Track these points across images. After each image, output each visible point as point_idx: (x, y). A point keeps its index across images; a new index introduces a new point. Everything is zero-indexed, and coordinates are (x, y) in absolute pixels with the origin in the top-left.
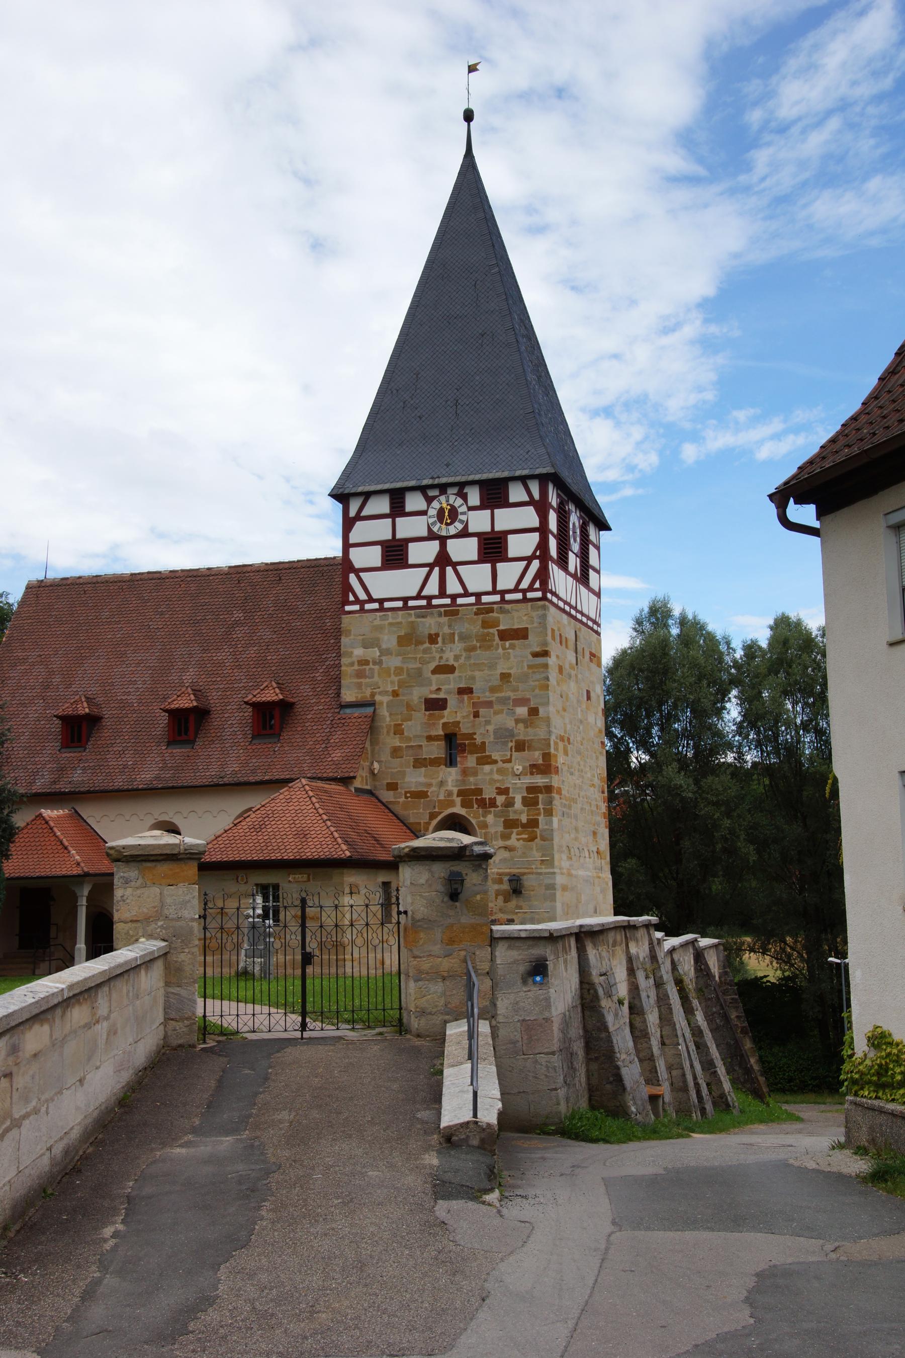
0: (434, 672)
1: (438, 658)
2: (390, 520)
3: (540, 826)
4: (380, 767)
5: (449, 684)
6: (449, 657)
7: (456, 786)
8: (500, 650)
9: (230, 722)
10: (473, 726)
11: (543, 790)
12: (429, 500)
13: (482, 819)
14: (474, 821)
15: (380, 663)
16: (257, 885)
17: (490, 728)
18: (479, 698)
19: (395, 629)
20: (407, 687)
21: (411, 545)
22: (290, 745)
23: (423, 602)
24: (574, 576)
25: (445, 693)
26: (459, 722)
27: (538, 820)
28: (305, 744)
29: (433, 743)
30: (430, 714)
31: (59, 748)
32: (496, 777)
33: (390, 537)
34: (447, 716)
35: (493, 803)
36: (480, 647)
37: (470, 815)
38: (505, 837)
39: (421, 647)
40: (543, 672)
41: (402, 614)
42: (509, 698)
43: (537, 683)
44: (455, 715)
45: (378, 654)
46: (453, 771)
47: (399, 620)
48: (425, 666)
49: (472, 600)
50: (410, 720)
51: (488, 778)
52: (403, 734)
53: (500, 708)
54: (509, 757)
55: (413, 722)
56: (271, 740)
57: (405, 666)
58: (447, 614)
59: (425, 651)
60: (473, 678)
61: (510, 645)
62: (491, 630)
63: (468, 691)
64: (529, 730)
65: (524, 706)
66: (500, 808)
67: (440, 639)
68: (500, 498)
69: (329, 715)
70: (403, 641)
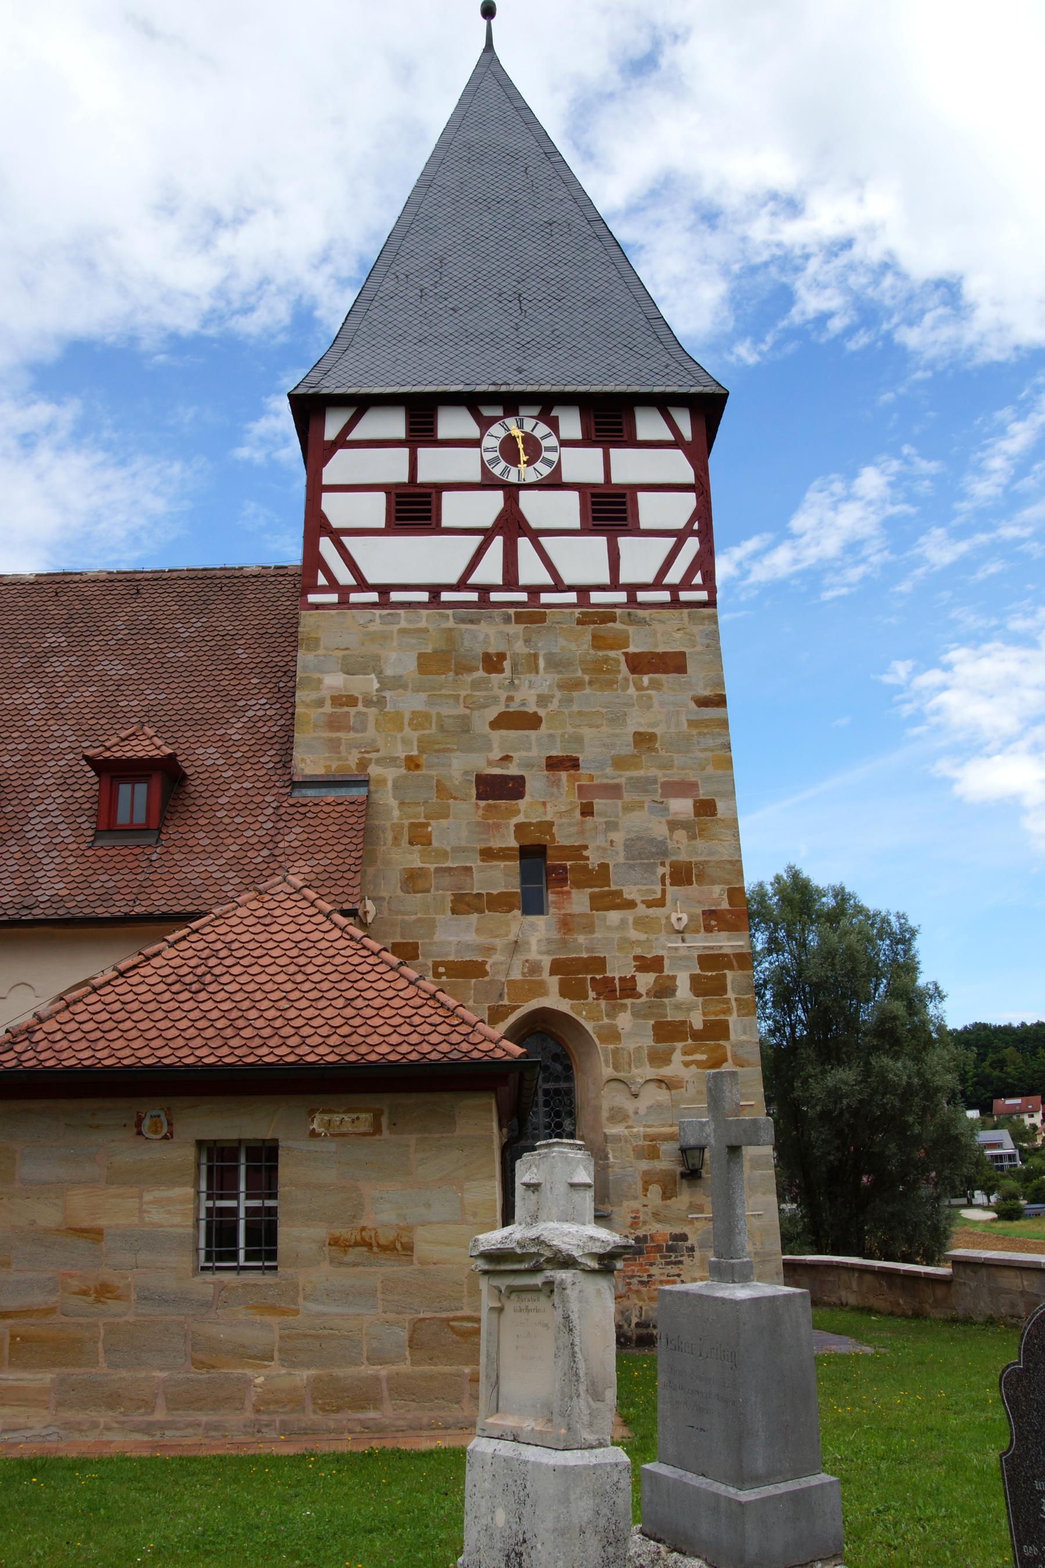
0: (495, 725)
1: (503, 698)
2: (405, 451)
4: (379, 911)
5: (529, 749)
7: (548, 953)
8: (632, 690)
9: (42, 807)
10: (582, 832)
11: (735, 963)
12: (484, 424)
13: (606, 1021)
14: (589, 1026)
15: (381, 702)
16: (200, 1144)
17: (618, 837)
18: (591, 777)
19: (414, 641)
20: (438, 751)
21: (446, 496)
22: (186, 849)
23: (473, 596)
25: (519, 765)
26: (551, 824)
27: (727, 1021)
28: (222, 848)
29: (495, 863)
30: (489, 806)
32: (634, 934)
33: (405, 479)
35: (629, 988)
36: (590, 683)
37: (580, 1014)
38: (659, 1058)
39: (468, 678)
40: (720, 735)
41: (428, 615)
42: (655, 782)
43: (709, 754)
44: (541, 809)
45: (376, 685)
46: (539, 920)
47: (423, 624)
48: (476, 712)
49: (572, 597)
50: (447, 817)
51: (616, 936)
52: (430, 844)
53: (637, 798)
54: (659, 896)
55: (451, 819)
56: (139, 841)
57: (433, 711)
58: (519, 618)
59: (476, 685)
60: (579, 740)
61: (651, 681)
62: (612, 654)
63: (573, 763)
64: (700, 844)
65: (686, 796)
66: (644, 999)
67: (507, 664)
68: (621, 431)
69: (268, 799)
70: (425, 664)
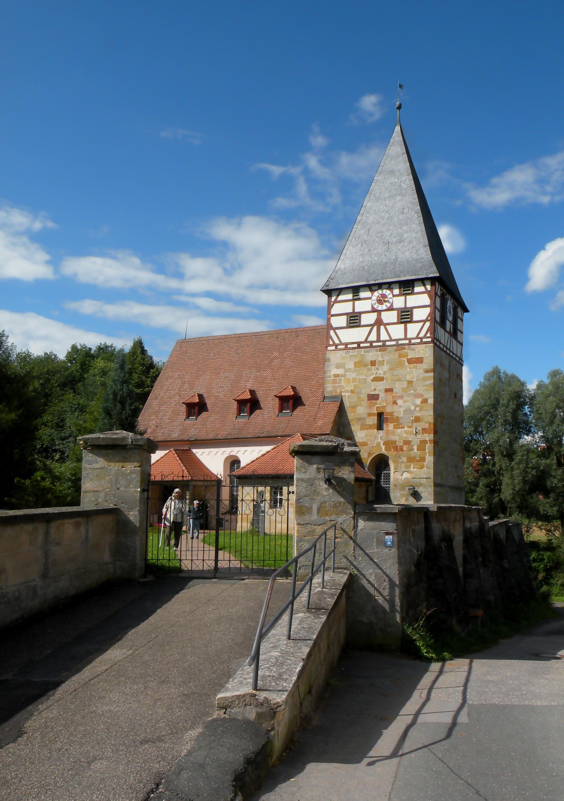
0: (373, 380)
3: (426, 461)
6: (381, 372)
8: (408, 369)
24: (449, 333)
29: (371, 417)
31: (184, 419)
33: (352, 311)
34: (380, 403)
62: (403, 359)
